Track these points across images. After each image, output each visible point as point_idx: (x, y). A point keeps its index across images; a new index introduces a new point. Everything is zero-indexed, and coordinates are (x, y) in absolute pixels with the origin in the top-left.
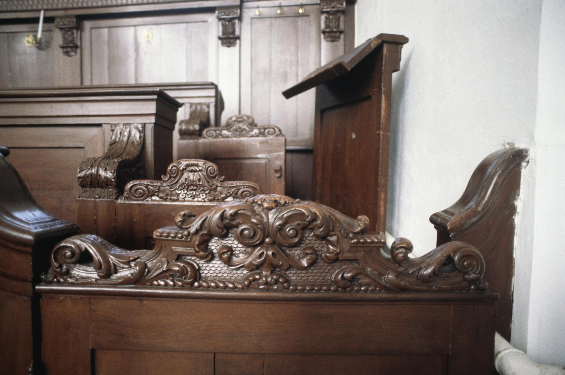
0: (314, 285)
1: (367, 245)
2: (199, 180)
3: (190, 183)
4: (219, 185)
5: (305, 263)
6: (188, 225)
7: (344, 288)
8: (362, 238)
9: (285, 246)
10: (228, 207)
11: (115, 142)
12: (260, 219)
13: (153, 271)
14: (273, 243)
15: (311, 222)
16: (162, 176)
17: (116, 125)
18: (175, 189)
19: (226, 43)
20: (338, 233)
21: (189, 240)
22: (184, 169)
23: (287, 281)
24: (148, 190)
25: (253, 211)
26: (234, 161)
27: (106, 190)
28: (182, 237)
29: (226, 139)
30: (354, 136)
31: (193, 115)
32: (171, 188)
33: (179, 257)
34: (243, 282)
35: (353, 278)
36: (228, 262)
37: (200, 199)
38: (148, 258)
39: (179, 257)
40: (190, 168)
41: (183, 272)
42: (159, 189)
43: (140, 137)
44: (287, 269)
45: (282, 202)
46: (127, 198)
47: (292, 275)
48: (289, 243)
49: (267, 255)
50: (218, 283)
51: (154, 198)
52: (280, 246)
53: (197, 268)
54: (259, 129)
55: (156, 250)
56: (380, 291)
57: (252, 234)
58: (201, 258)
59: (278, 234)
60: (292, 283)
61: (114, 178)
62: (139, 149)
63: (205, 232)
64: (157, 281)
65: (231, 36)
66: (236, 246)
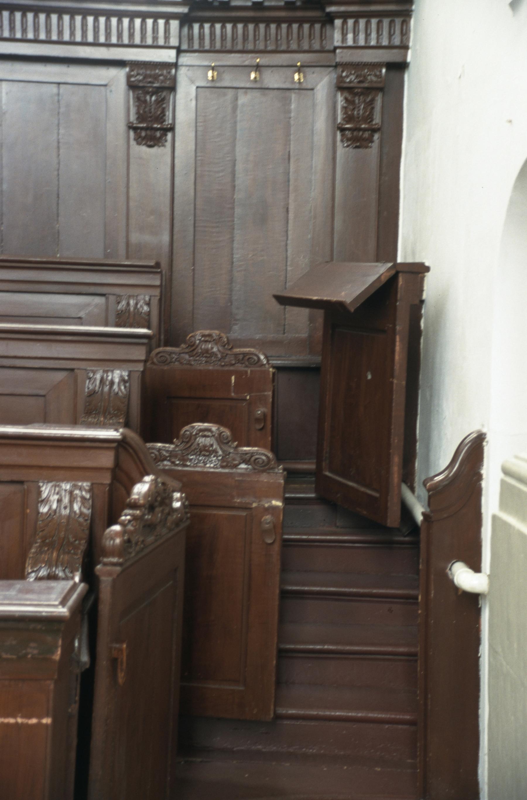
4: (232, 451)
18: (188, 454)
19: (144, 138)
51: (165, 463)
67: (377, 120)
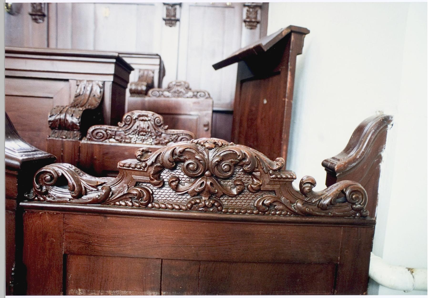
0: (241, 209)
1: (282, 180)
2: (148, 128)
3: (141, 130)
5: (234, 191)
6: (145, 158)
7: (264, 212)
8: (279, 174)
9: (221, 178)
10: (178, 146)
11: (80, 95)
12: (202, 156)
13: (116, 194)
14: (211, 176)
15: (241, 160)
16: (119, 123)
17: (80, 81)
19: (169, 23)
20: (261, 170)
21: (146, 170)
22: (136, 119)
23: (221, 205)
24: (107, 134)
25: (197, 150)
26: (172, 116)
27: (72, 132)
28: (140, 168)
29: (167, 99)
30: (265, 102)
31: (141, 78)
32: (125, 133)
33: (137, 184)
34: (187, 205)
35: (271, 204)
36: (176, 189)
37: (148, 143)
38: (112, 184)
39: (137, 184)
40: (141, 118)
41: (140, 196)
42: (115, 133)
43: (100, 92)
44: (222, 196)
45: (220, 144)
46: (89, 139)
47: (225, 201)
48: (223, 176)
49: (206, 184)
50: (167, 205)
51: (111, 140)
52: (217, 178)
53: (151, 193)
54: (193, 92)
55: (119, 177)
56: (290, 215)
57: (195, 167)
58: (155, 185)
59: (216, 169)
60: (224, 207)
61: (79, 123)
62: (99, 101)
63: (159, 164)
64: (119, 201)
65: (173, 18)
66: (182, 177)
67: (259, 18)
